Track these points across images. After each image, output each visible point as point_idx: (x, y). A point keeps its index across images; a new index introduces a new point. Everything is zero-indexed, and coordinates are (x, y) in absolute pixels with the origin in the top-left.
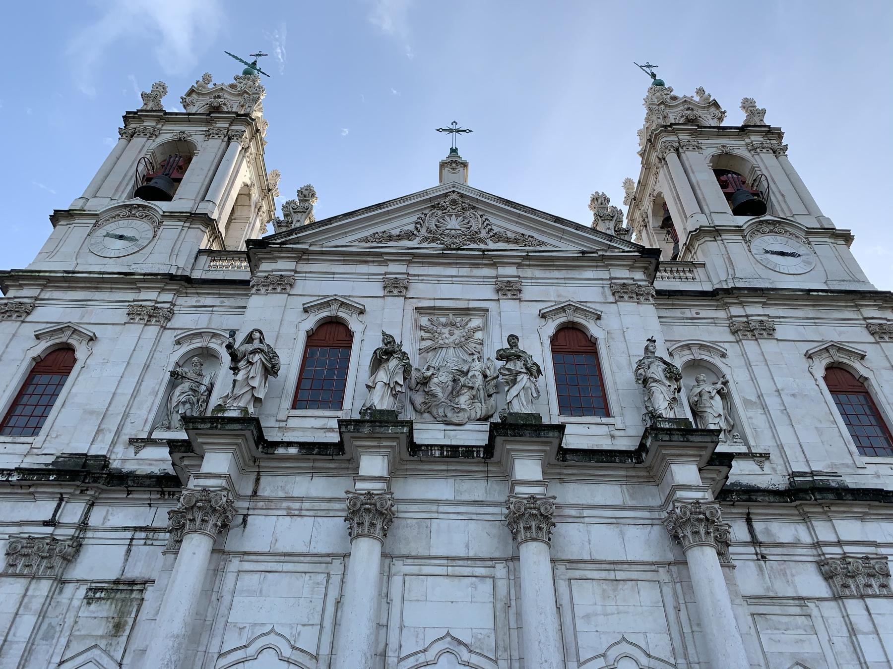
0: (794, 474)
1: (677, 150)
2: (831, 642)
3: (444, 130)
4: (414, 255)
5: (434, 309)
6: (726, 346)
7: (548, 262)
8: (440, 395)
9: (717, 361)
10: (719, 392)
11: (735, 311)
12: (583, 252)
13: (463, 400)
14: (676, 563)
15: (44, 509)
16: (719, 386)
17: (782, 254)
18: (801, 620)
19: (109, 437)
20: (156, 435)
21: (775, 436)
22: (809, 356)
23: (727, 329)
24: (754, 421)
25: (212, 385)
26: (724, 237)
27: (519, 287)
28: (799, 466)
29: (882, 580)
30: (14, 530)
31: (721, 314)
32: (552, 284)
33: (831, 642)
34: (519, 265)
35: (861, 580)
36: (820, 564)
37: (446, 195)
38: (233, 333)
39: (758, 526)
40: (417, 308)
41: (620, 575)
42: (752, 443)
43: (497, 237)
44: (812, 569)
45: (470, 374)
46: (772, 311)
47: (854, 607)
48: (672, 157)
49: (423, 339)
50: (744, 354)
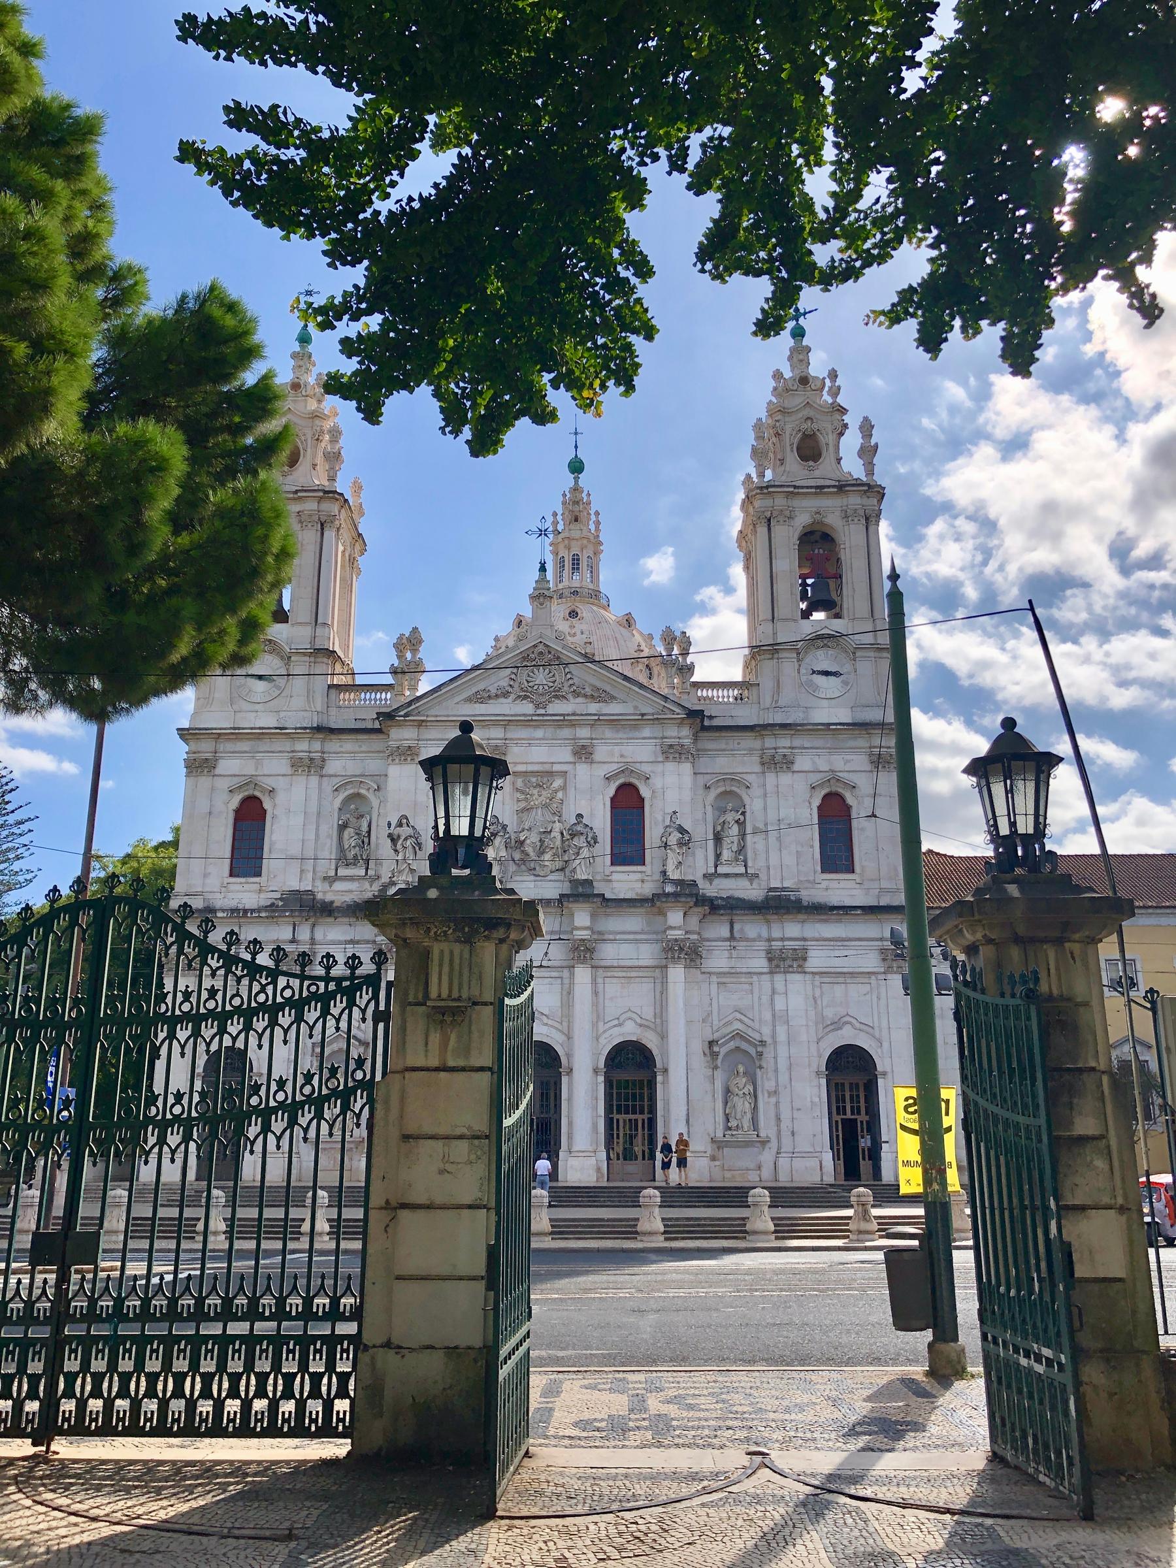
0: (771, 890)
1: (769, 520)
2: (760, 998)
3: (534, 533)
6: (751, 778)
7: (614, 722)
8: (532, 854)
9: (742, 792)
10: (737, 822)
11: (769, 742)
12: (643, 715)
13: (547, 857)
16: (738, 816)
17: (827, 673)
18: (747, 987)
19: (310, 875)
20: (341, 872)
21: (767, 859)
23: (758, 759)
24: (757, 846)
25: (369, 826)
26: (781, 655)
27: (590, 750)
28: (775, 884)
29: (801, 962)
31: (757, 744)
32: (617, 744)
33: (760, 998)
35: (789, 962)
36: (769, 952)
37: (535, 646)
38: (389, 825)
39: (737, 927)
41: (634, 974)
42: (750, 864)
43: (576, 694)
44: (763, 954)
45: (553, 834)
46: (797, 742)
47: (779, 978)
48: (762, 530)
49: (518, 801)
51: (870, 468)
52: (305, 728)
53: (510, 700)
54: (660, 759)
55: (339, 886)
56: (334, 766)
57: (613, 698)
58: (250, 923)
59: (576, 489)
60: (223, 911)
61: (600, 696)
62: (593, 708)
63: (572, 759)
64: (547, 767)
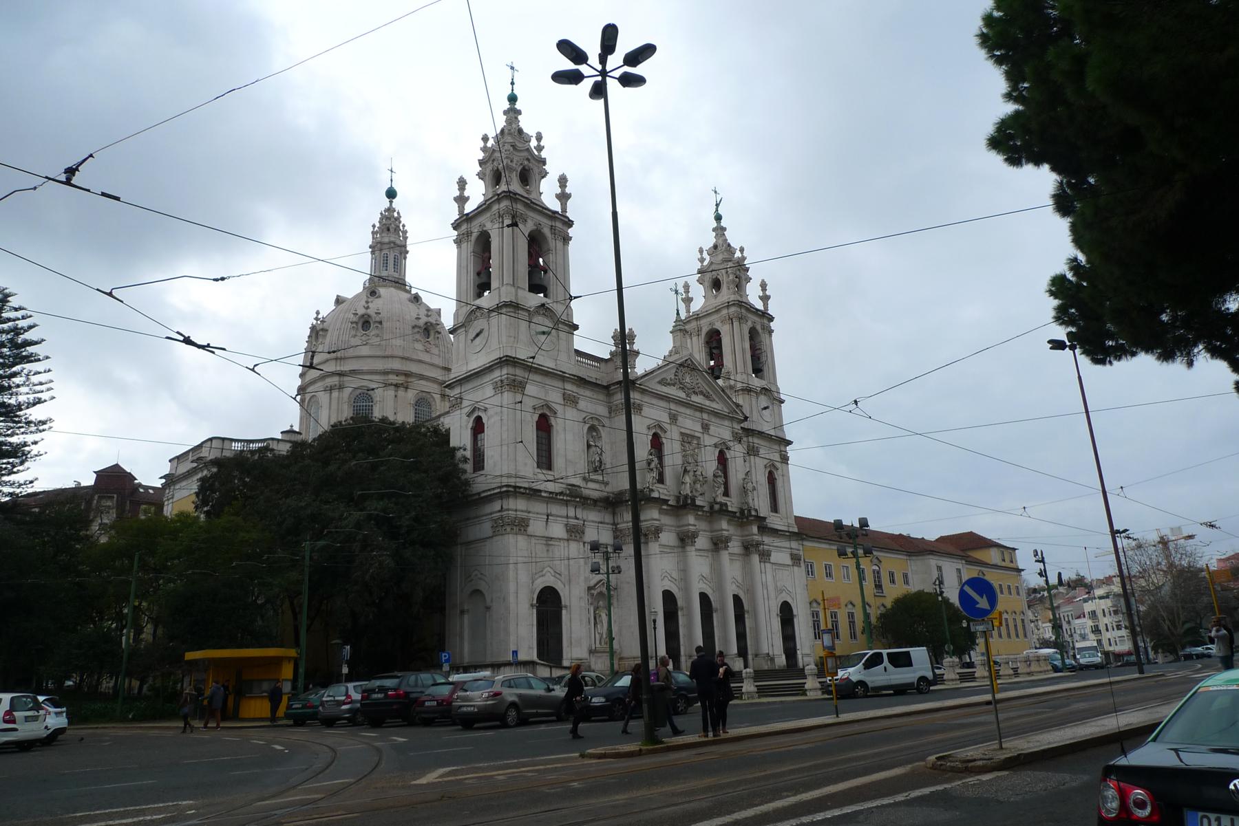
4: (680, 401)
5: (685, 434)
7: (716, 414)
11: (750, 439)
14: (743, 555)
15: (571, 513)
20: (593, 477)
22: (765, 467)
30: (565, 520)
32: (718, 427)
34: (708, 413)
37: (687, 360)
40: (681, 433)
43: (702, 393)
48: (736, 324)
50: (750, 462)
51: (766, 305)
52: (575, 376)
53: (675, 388)
54: (732, 439)
55: (591, 485)
56: (582, 404)
57: (714, 400)
58: (554, 502)
59: (390, 210)
60: (546, 492)
61: (707, 397)
62: (707, 403)
63: (701, 431)
64: (692, 433)
